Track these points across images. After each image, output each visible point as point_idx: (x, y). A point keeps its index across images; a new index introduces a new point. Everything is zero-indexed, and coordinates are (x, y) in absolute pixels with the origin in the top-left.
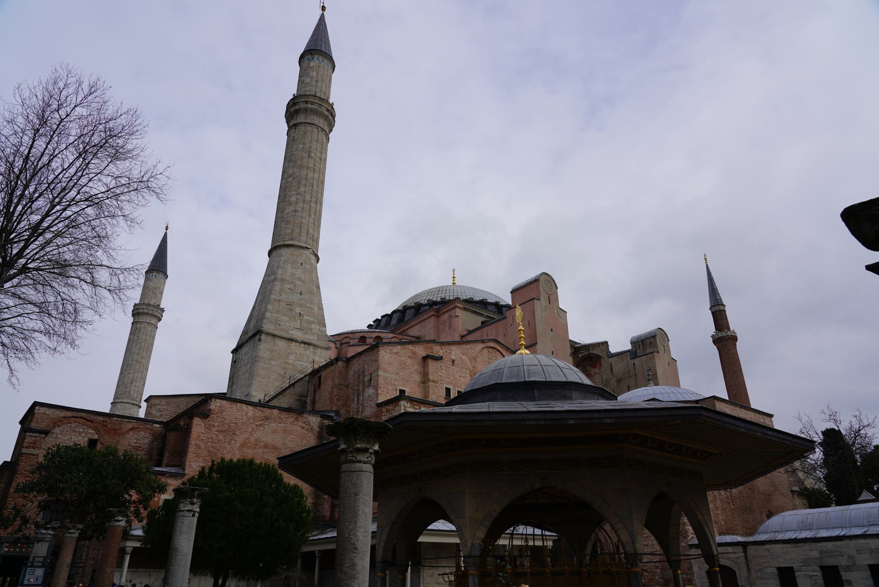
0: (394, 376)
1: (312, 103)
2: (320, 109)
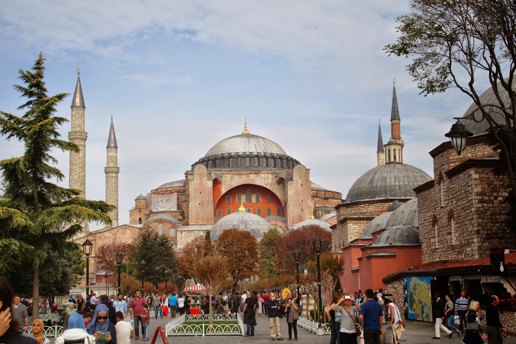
2: (76, 137)
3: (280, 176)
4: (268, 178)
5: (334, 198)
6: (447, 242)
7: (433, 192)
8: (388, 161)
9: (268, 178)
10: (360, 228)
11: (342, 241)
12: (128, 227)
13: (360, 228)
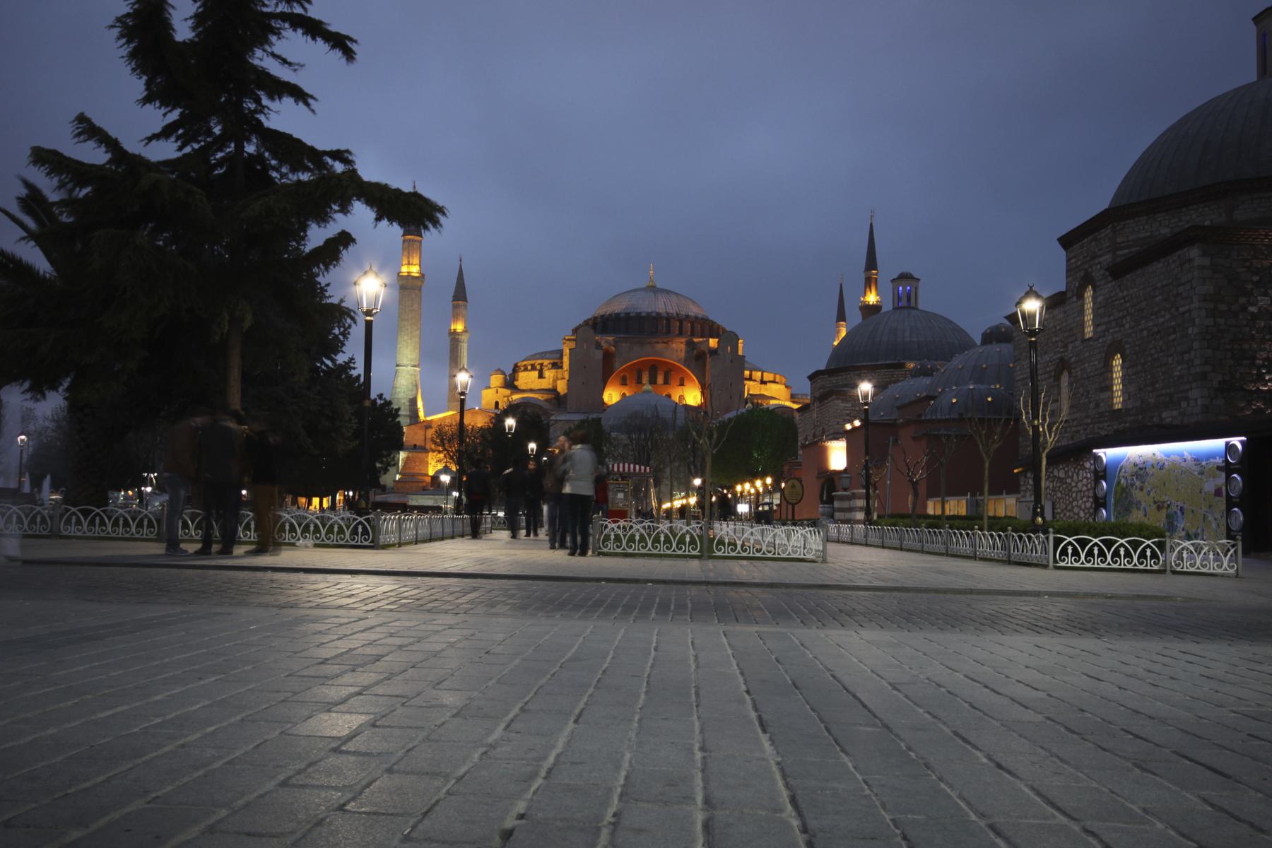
4: (681, 350)
5: (774, 382)
6: (1097, 405)
7: (1062, 315)
8: (896, 305)
9: (681, 350)
10: (853, 408)
11: (821, 428)
13: (853, 408)
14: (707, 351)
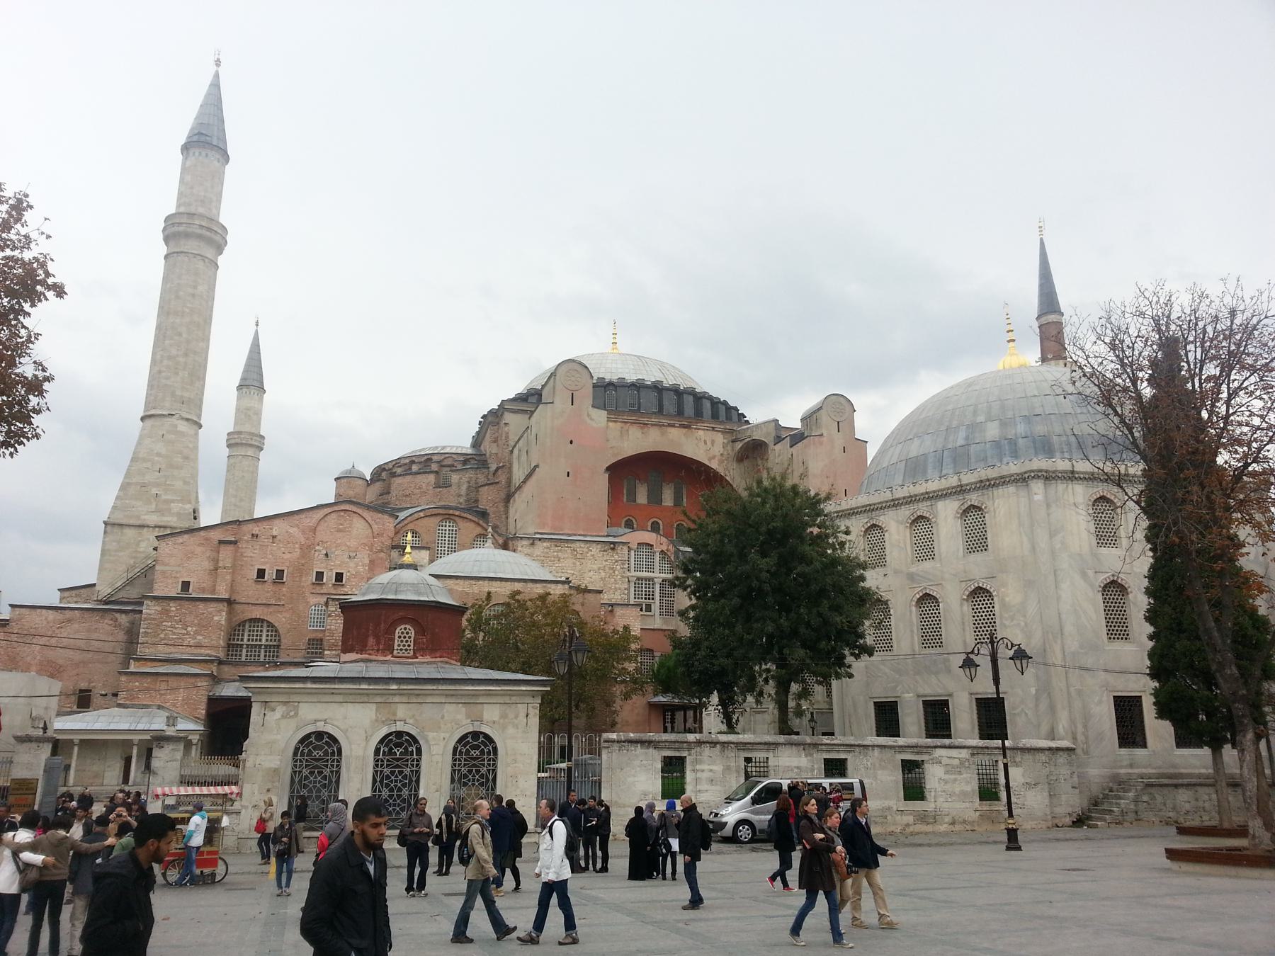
0: (177, 569)
1: (180, 224)
2: (189, 230)
3: (750, 437)
4: (713, 442)
9: (713, 442)
12: (359, 511)
14: (769, 440)
